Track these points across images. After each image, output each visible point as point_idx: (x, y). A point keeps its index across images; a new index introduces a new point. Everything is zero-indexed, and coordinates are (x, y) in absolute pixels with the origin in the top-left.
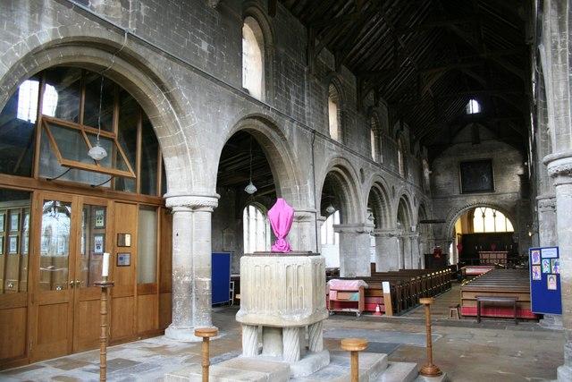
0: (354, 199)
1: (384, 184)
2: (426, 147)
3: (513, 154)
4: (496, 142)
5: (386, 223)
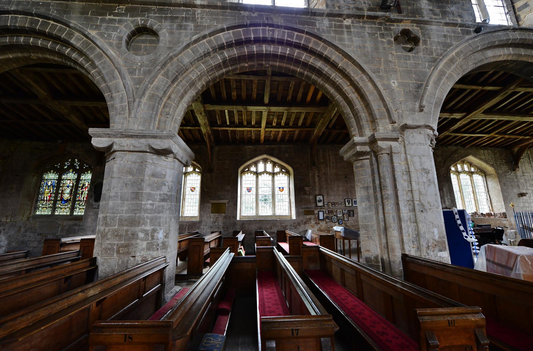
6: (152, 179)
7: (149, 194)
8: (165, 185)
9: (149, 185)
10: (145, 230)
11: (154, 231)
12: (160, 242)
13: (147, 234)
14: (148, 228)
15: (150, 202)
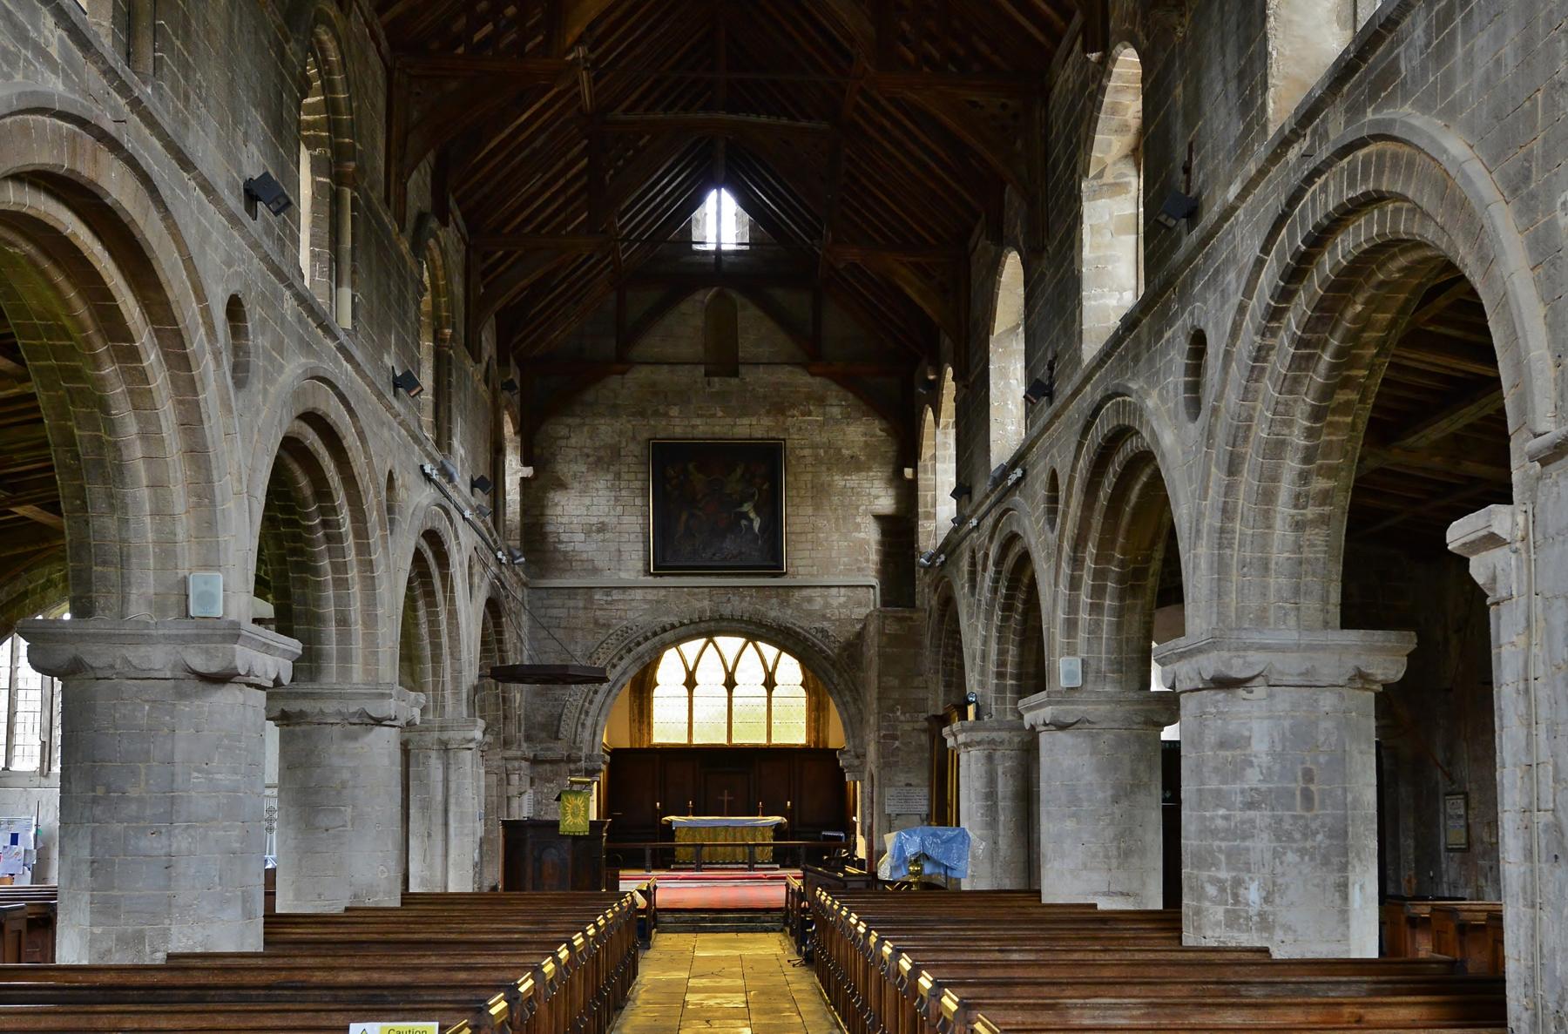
0: (178, 471)
1: (350, 440)
2: (519, 364)
3: (860, 433)
4: (804, 380)
5: (345, 657)
6: (1222, 753)
7: (1219, 791)
8: (1251, 764)
9: (1216, 770)
10: (1219, 881)
11: (1238, 883)
12: (1253, 911)
13: (1222, 890)
14: (1223, 874)
15: (1221, 812)
